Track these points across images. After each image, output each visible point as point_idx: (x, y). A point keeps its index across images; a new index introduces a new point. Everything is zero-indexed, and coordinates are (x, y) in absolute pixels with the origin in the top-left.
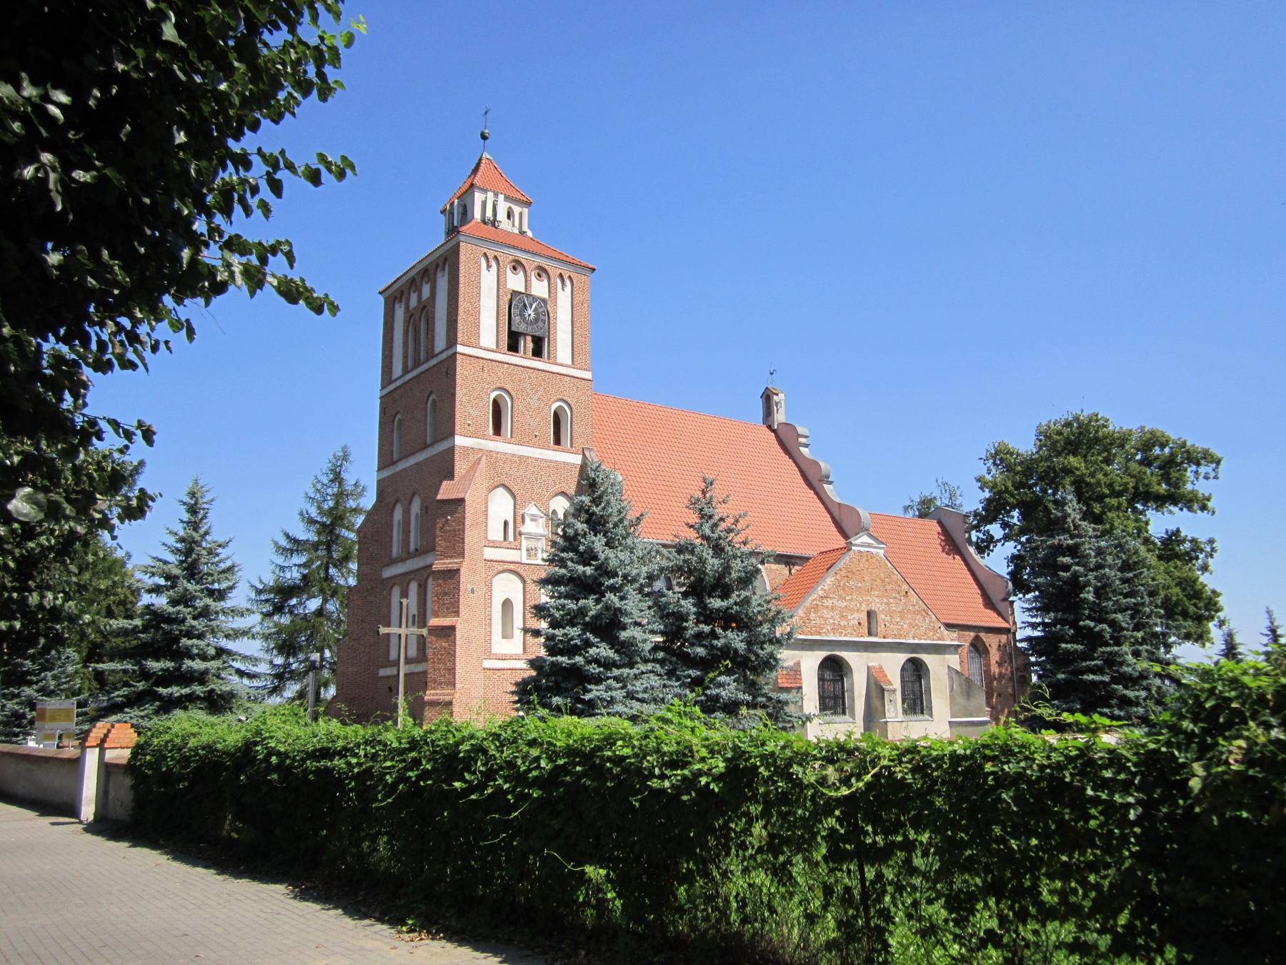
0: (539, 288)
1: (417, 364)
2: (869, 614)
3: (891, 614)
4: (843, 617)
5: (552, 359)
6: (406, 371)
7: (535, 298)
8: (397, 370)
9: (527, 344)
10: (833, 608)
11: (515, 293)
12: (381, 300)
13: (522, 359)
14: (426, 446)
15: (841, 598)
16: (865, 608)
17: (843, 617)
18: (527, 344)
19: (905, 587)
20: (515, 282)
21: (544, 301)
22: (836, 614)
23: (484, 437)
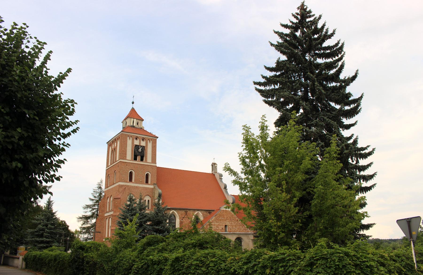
0: (143, 144)
1: (113, 163)
2: (226, 226)
3: (232, 226)
4: (217, 227)
5: (146, 161)
6: (111, 164)
7: (141, 146)
8: (109, 164)
9: (139, 158)
10: (214, 225)
11: (136, 145)
12: (107, 145)
13: (138, 162)
14: (114, 184)
15: (217, 222)
16: (224, 225)
17: (217, 227)
18: (139, 158)
19: (237, 219)
20: (137, 142)
21: (144, 147)
22: (215, 227)
23: (127, 182)
